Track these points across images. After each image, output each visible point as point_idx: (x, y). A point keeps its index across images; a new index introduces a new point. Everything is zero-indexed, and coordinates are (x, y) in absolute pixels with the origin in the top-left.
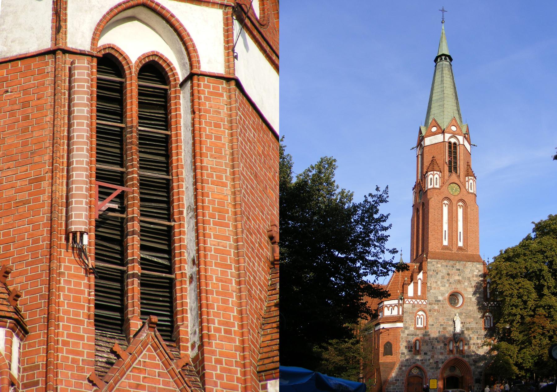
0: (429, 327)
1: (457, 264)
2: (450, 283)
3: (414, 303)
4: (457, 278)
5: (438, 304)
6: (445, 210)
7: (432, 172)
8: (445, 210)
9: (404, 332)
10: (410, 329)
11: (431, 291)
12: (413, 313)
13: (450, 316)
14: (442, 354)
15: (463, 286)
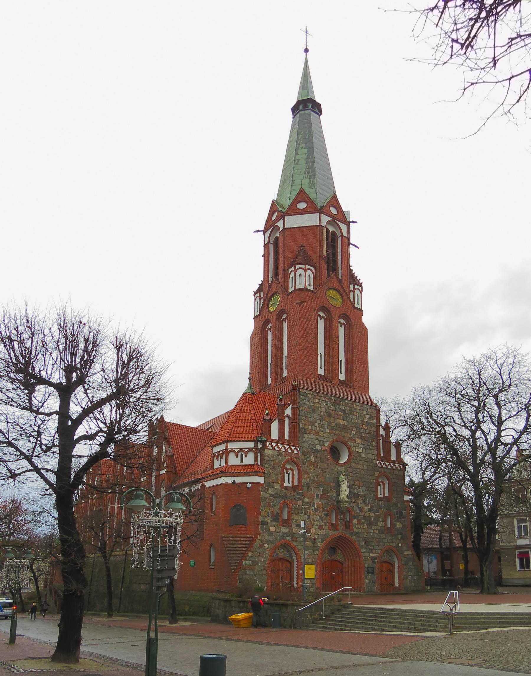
3: (280, 449)
4: (341, 422)
11: (306, 435)
14: (321, 528)
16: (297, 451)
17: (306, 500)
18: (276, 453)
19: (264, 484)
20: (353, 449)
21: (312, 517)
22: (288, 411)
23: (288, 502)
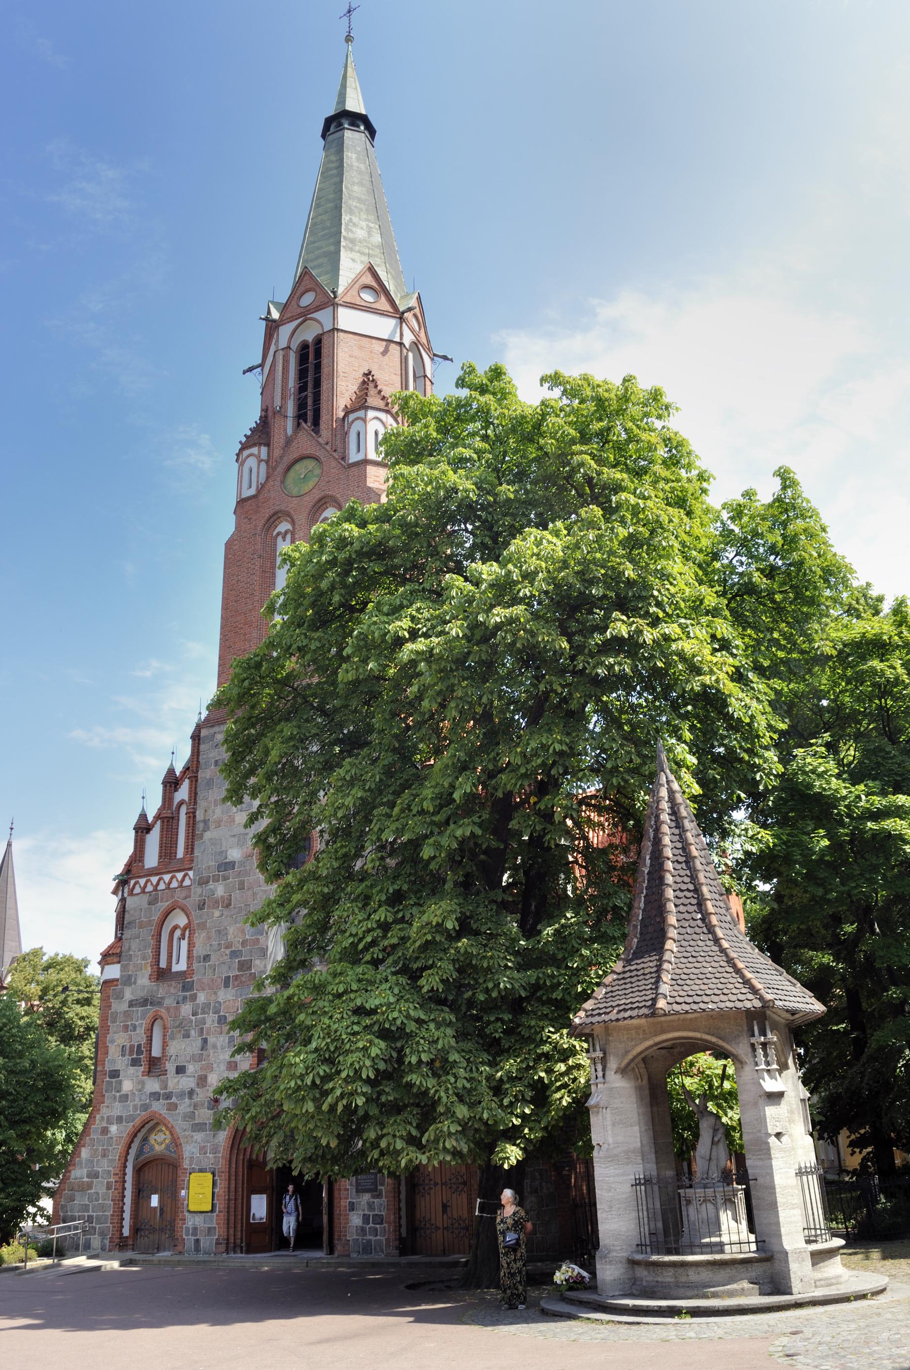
5: (225, 878)
10: (139, 982)
11: (207, 835)
18: (145, 898)
21: (211, 1040)
23: (163, 1012)
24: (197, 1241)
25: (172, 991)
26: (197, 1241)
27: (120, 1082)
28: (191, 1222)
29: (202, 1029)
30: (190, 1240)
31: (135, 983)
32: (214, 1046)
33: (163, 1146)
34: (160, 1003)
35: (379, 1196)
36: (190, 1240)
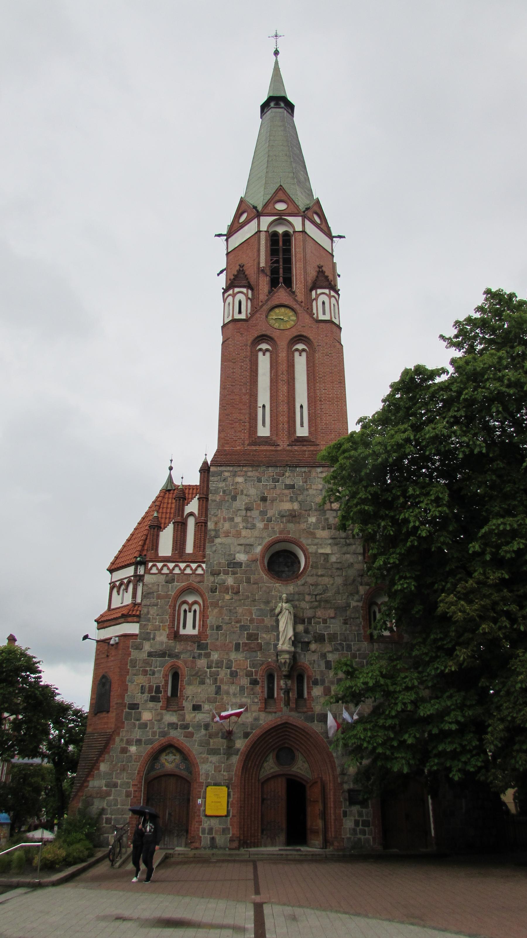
0: (209, 632)
1: (287, 474)
2: (270, 520)
4: (287, 506)
5: (234, 573)
6: (264, 363)
7: (231, 292)
8: (264, 363)
9: (139, 648)
10: (158, 639)
11: (218, 541)
12: (167, 596)
13: (267, 603)
15: (303, 526)
16: (203, 569)
17: (215, 656)
18: (162, 578)
19: (136, 635)
20: (312, 549)
21: (224, 687)
22: (193, 506)
23: (180, 663)
24: (213, 839)
25: (189, 648)
26: (213, 839)
27: (140, 713)
28: (206, 824)
29: (216, 679)
30: (206, 839)
31: (154, 639)
32: (228, 693)
33: (173, 765)
34: (177, 656)
35: (367, 807)
36: (206, 839)
